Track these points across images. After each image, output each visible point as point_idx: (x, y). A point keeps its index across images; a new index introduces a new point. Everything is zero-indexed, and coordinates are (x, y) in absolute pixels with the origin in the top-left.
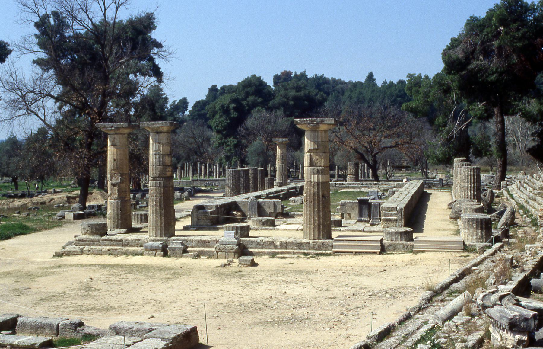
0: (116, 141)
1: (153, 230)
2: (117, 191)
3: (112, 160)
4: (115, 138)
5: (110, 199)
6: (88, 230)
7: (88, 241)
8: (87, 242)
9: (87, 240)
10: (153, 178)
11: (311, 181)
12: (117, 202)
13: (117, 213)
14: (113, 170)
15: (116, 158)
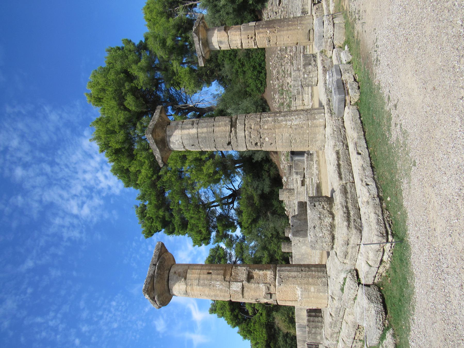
0: (179, 270)
1: (315, 119)
2: (261, 273)
3: (209, 276)
4: (175, 273)
5: (275, 286)
6: (323, 207)
7: (347, 202)
8: (349, 205)
9: (344, 204)
10: (232, 126)
11: (255, 26)
12: (279, 271)
13: (298, 271)
14: (225, 278)
15: (206, 271)
